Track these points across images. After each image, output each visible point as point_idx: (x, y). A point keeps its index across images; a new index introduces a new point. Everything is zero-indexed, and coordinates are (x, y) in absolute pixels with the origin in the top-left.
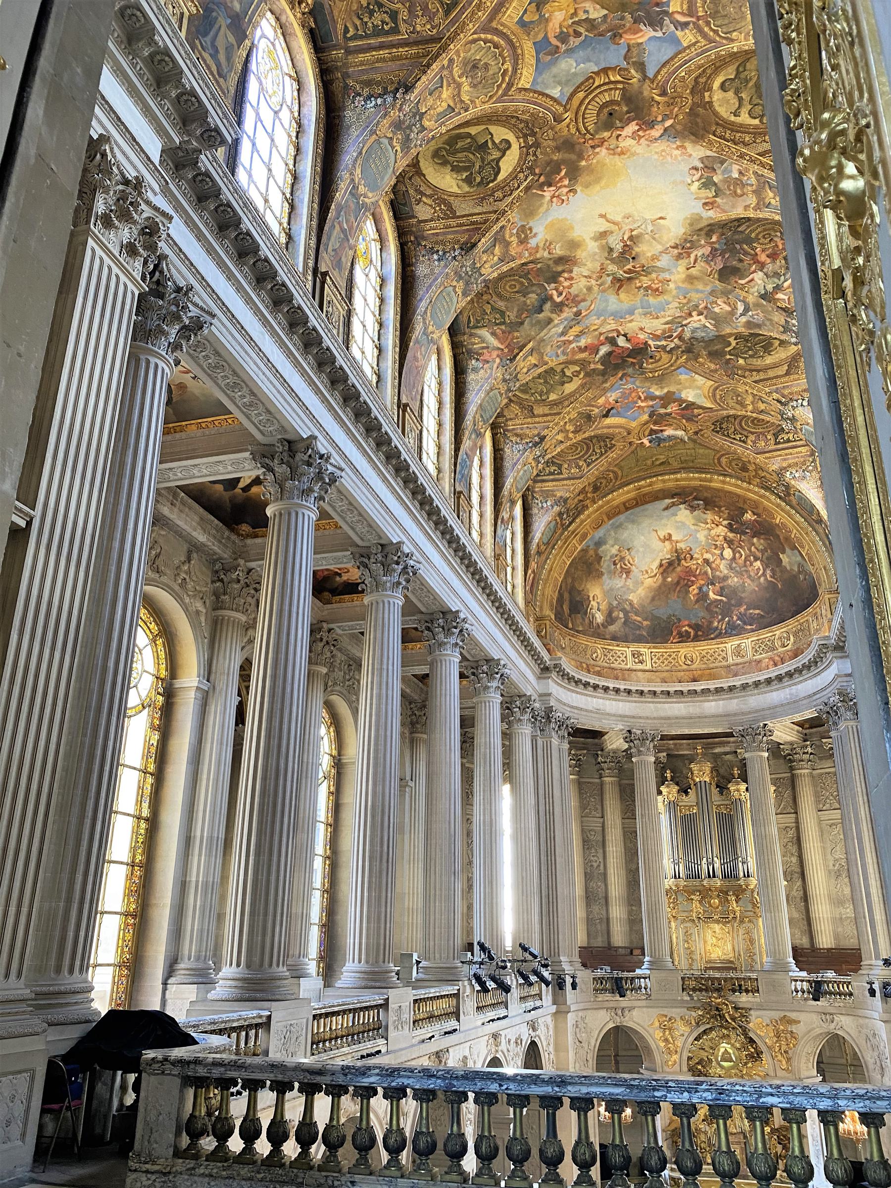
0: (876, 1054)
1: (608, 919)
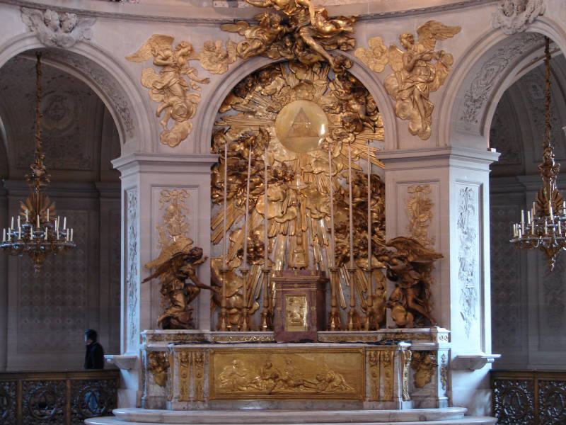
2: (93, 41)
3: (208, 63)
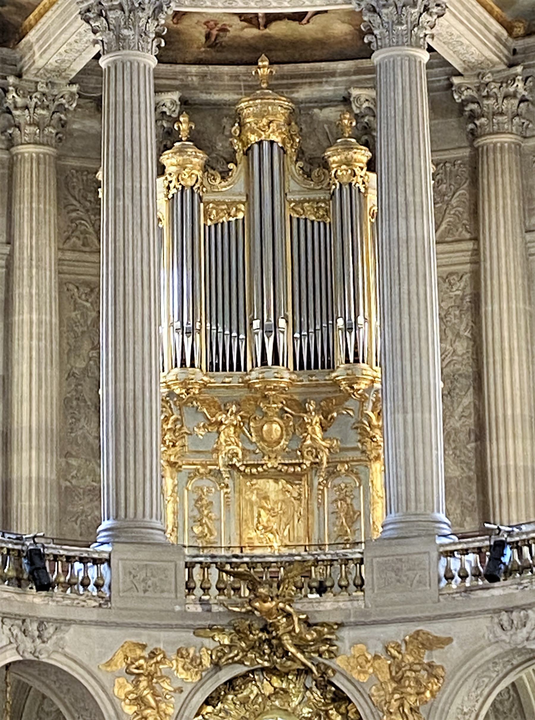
2: (67, 650)
3: (181, 670)
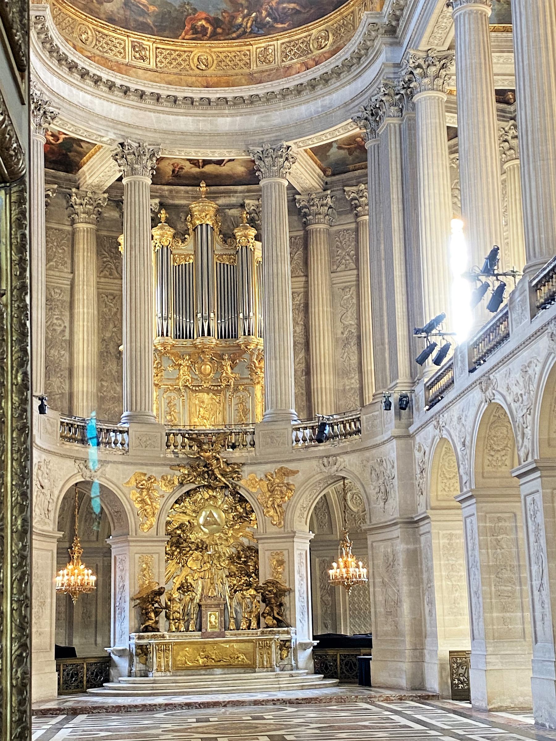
0: (381, 481)
1: (71, 395)
2: (107, 476)
